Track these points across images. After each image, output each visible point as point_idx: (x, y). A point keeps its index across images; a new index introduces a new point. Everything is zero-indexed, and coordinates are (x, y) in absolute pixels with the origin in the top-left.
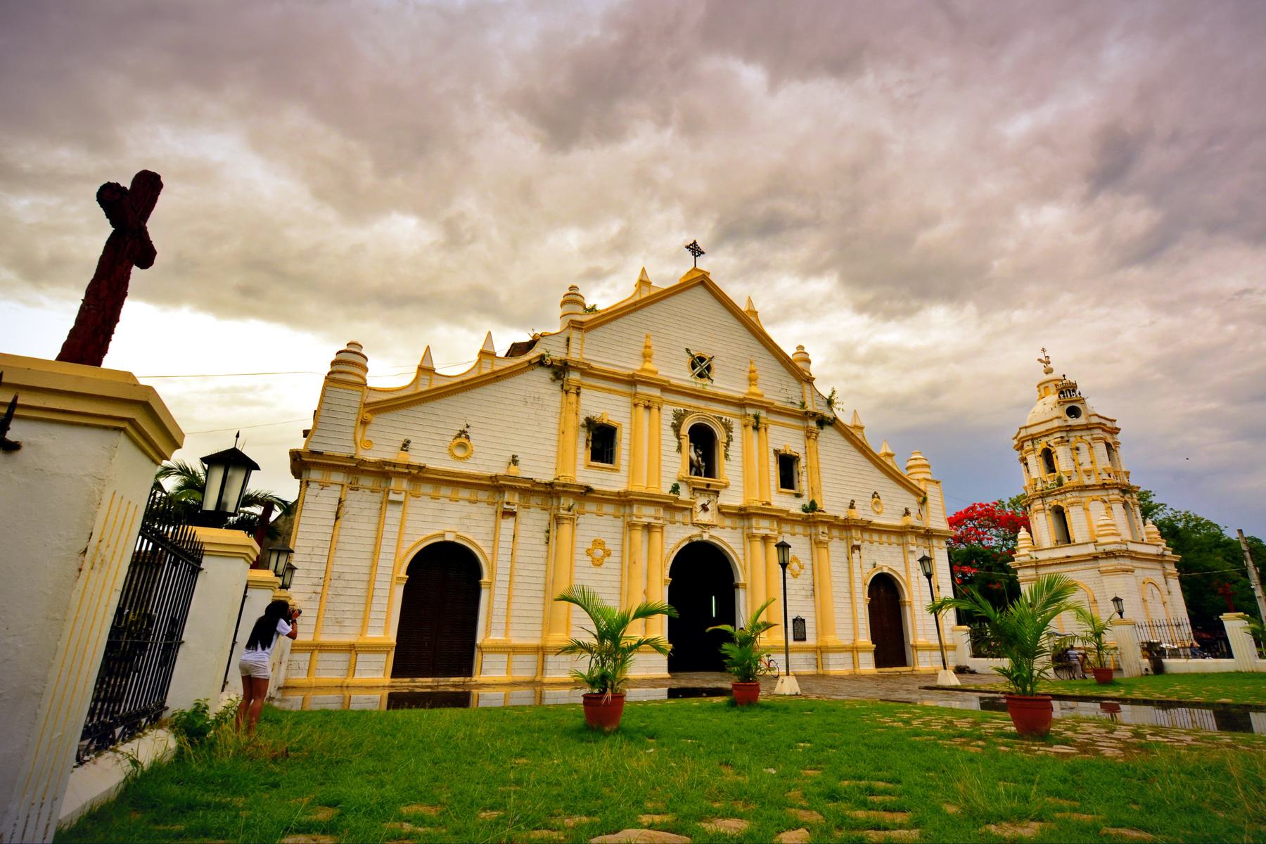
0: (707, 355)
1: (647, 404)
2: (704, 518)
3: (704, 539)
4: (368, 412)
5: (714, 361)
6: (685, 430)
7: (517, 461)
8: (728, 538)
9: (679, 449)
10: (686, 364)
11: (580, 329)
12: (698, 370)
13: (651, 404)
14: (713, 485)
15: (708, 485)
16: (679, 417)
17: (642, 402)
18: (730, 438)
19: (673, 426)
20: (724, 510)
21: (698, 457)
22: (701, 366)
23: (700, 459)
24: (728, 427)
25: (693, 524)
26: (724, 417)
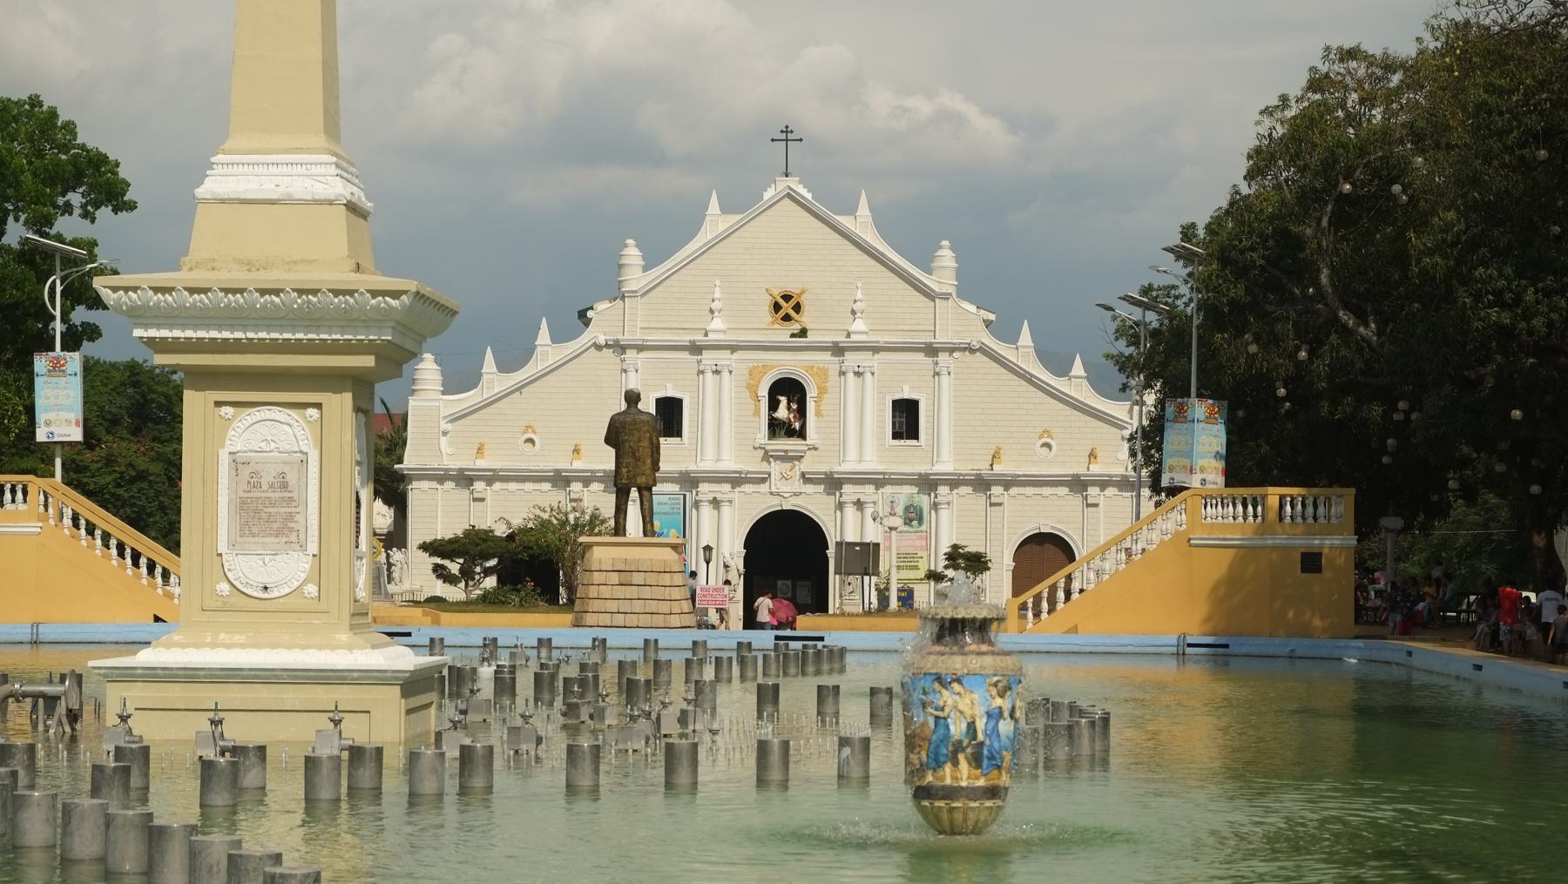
0: (792, 289)
1: (714, 368)
2: (784, 488)
3: (784, 508)
4: (446, 423)
5: (804, 297)
6: (764, 392)
7: (579, 450)
8: (816, 505)
9: (757, 413)
10: (767, 308)
11: (634, 297)
12: (782, 313)
13: (719, 368)
14: (791, 451)
15: (786, 451)
16: (755, 374)
17: (708, 367)
18: (822, 391)
19: (749, 387)
20: (807, 476)
21: (789, 413)
22: (786, 307)
23: (792, 416)
24: (822, 374)
25: (771, 493)
26: (816, 366)
